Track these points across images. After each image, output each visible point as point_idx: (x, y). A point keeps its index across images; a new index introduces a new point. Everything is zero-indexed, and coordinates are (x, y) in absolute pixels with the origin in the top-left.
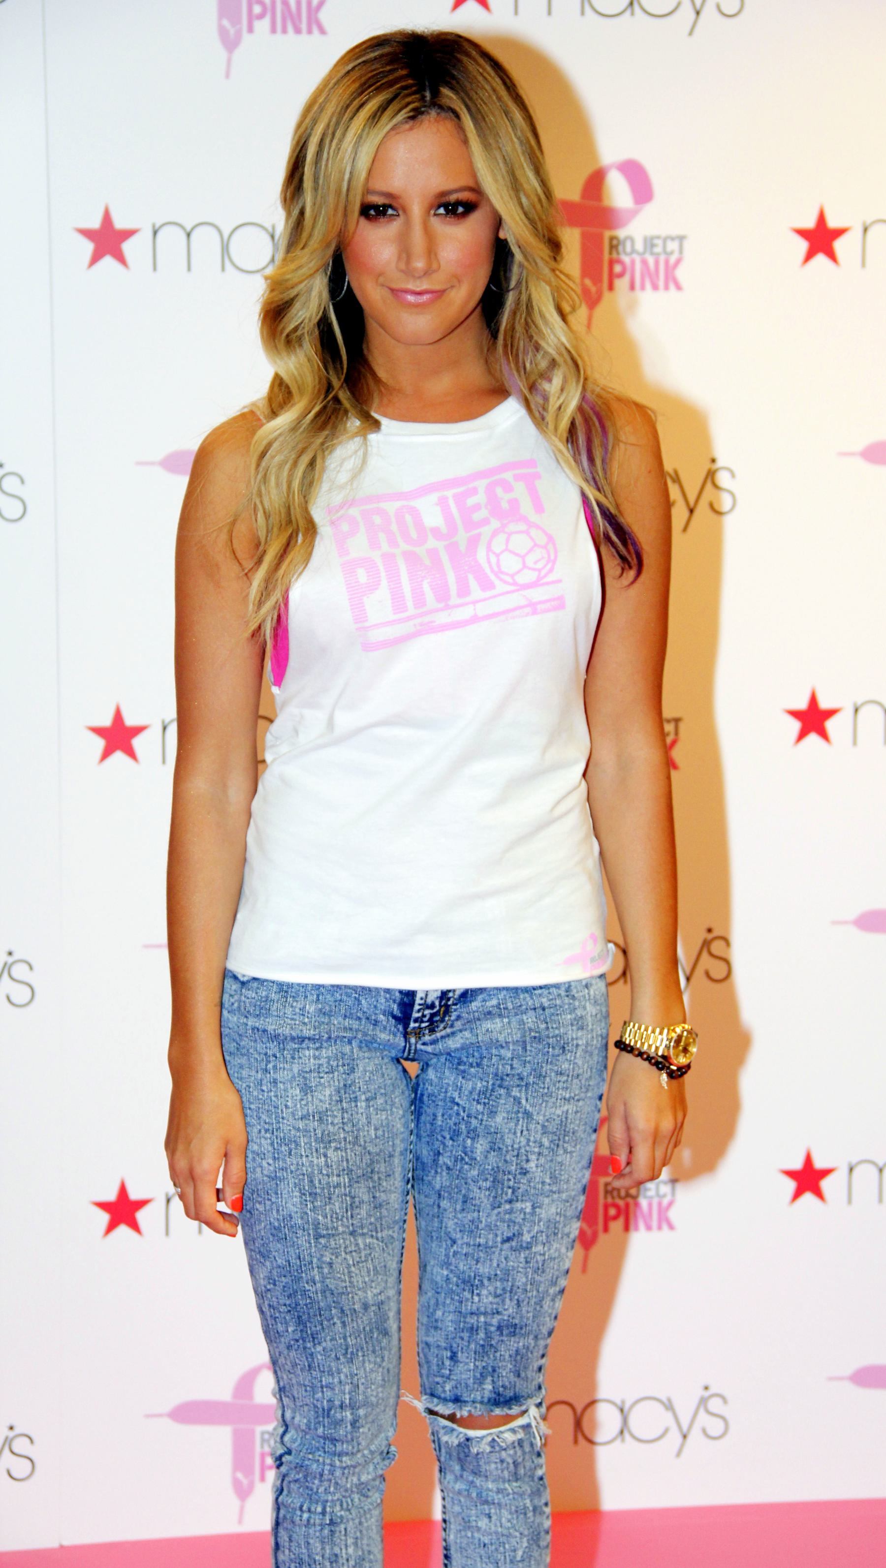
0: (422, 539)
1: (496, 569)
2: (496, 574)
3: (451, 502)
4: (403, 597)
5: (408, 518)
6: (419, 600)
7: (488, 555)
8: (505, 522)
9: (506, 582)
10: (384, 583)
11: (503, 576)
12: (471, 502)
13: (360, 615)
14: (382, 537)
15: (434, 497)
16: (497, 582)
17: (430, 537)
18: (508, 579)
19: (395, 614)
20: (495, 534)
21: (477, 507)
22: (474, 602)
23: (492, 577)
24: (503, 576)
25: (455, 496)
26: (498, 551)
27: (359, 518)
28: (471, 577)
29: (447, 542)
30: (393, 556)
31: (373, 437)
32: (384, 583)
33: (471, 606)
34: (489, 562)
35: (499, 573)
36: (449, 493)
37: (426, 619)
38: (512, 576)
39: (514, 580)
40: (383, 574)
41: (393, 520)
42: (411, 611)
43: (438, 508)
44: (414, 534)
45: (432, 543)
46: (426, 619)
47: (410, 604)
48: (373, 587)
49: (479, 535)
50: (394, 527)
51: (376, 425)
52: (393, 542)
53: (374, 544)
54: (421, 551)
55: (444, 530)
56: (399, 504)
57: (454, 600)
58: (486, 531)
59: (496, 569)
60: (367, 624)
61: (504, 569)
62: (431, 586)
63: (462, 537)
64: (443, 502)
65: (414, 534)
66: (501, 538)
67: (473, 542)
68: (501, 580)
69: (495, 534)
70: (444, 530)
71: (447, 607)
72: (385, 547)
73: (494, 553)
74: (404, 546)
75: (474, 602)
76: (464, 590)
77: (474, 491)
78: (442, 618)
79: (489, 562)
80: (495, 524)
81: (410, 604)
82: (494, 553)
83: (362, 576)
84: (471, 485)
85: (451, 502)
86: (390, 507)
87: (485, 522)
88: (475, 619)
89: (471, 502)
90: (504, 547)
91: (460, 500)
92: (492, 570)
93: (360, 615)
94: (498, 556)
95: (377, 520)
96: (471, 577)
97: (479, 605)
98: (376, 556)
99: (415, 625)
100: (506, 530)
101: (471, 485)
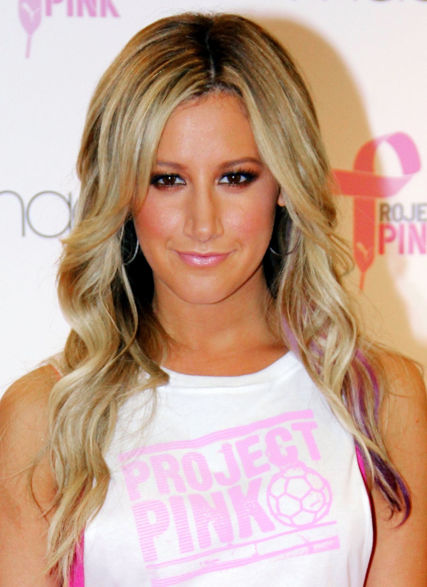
0: (207, 484)
1: (275, 511)
2: (275, 516)
3: (234, 450)
4: (190, 537)
5: (195, 465)
7: (268, 499)
9: (285, 524)
10: (172, 524)
11: (282, 518)
12: (252, 449)
13: (150, 553)
14: (170, 482)
15: (218, 445)
17: (215, 481)
18: (288, 521)
19: (182, 552)
20: (275, 478)
21: (258, 454)
22: (256, 542)
23: (272, 519)
24: (282, 518)
25: (237, 444)
26: (277, 494)
27: (149, 465)
29: (230, 487)
30: (181, 499)
31: (162, 389)
32: (172, 524)
33: (253, 546)
35: (278, 515)
36: (232, 441)
37: (211, 558)
38: (291, 518)
39: (292, 521)
41: (181, 466)
42: (197, 549)
43: (222, 456)
44: (200, 479)
45: (216, 487)
46: (211, 558)
47: (196, 544)
48: (162, 527)
49: (260, 480)
50: (181, 473)
51: (165, 378)
52: (180, 487)
53: (163, 488)
54: (206, 494)
55: (228, 475)
56: (185, 451)
57: (237, 540)
58: (266, 476)
59: (275, 511)
61: (283, 511)
62: (215, 527)
63: (244, 482)
64: (226, 449)
65: (200, 479)
66: (280, 484)
67: (255, 487)
68: (281, 522)
69: (275, 478)
70: (228, 475)
71: (231, 547)
72: (173, 491)
73: (274, 497)
74: (190, 490)
75: (256, 542)
76: (246, 531)
77: (256, 439)
78: (226, 557)
80: (275, 470)
81: (196, 544)
82: (274, 497)
83: (152, 518)
85: (234, 450)
86: (179, 454)
87: (265, 468)
88: (256, 558)
89: (252, 449)
90: (283, 491)
91: (242, 447)
92: (272, 513)
93: (150, 553)
94: (277, 499)
95: (166, 466)
97: (259, 545)
98: (165, 499)
99: (201, 563)
100: (285, 475)
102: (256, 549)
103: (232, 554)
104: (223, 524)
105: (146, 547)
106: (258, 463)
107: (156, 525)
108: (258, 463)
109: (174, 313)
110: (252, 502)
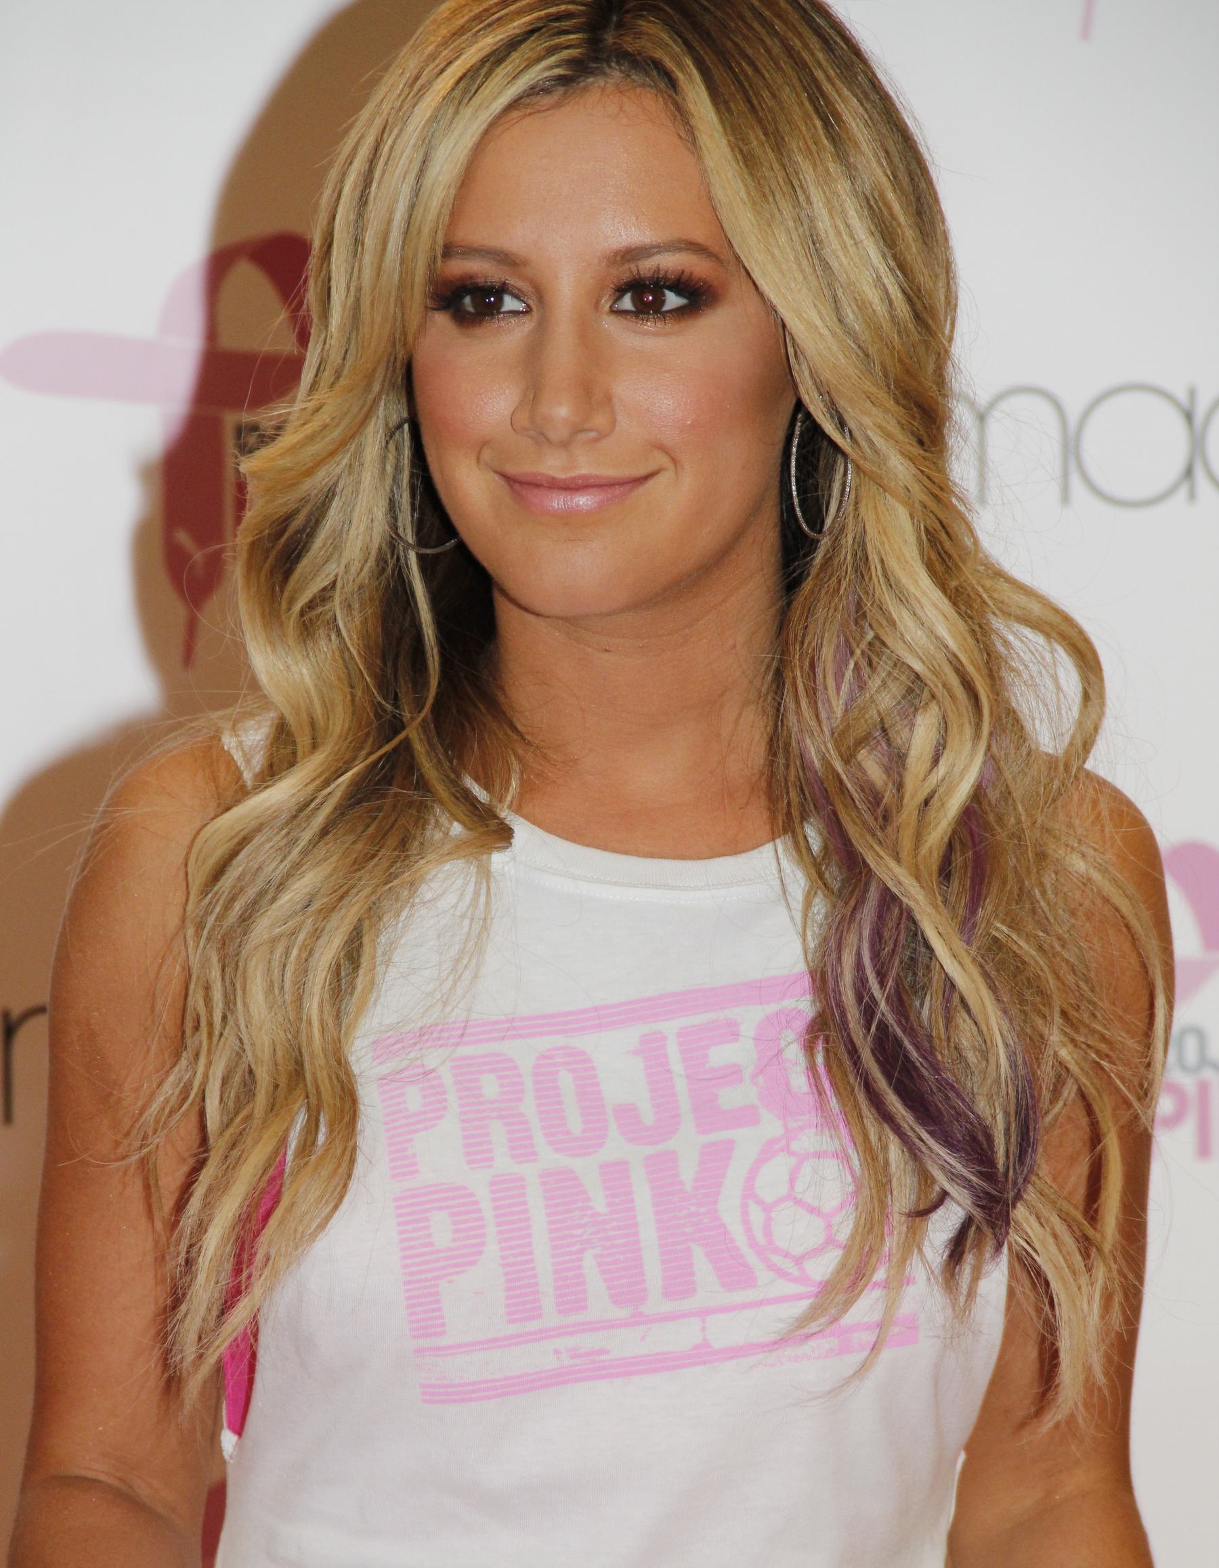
1: (761, 1239)
3: (673, 1050)
5: (566, 1081)
6: (571, 1295)
7: (744, 1206)
8: (793, 1125)
9: (782, 1274)
10: (492, 1248)
11: (777, 1259)
12: (721, 1055)
13: (426, 1318)
14: (498, 1132)
15: (630, 1036)
16: (763, 1275)
17: (613, 1125)
18: (788, 1266)
19: (511, 1322)
20: (767, 1153)
21: (732, 1074)
22: (704, 1313)
23: (752, 1259)
24: (777, 1259)
25: (681, 1034)
27: (447, 1078)
28: (698, 1252)
29: (650, 1150)
32: (492, 1248)
33: (696, 1322)
34: (746, 1222)
36: (670, 1027)
37: (588, 1341)
39: (802, 1270)
40: (491, 1230)
42: (551, 1317)
44: (575, 1124)
45: (615, 1147)
46: (588, 1341)
47: (548, 1302)
49: (729, 1145)
50: (529, 1106)
51: (504, 835)
52: (522, 1149)
53: (477, 1152)
54: (587, 1169)
55: (648, 1116)
56: (543, 1043)
57: (656, 1304)
58: (747, 1141)
59: (761, 1239)
60: (442, 1341)
62: (600, 1264)
63: (687, 1144)
64: (651, 1049)
65: (575, 1124)
66: (779, 1167)
67: (716, 1159)
68: (772, 1267)
69: (767, 1153)
70: (648, 1116)
71: (639, 1319)
72: (503, 1162)
73: (760, 1202)
74: (549, 1157)
75: (704, 1313)
76: (679, 1283)
77: (731, 1032)
79: (746, 1222)
80: (770, 1126)
81: (548, 1302)
82: (760, 1202)
83: (441, 1230)
84: (725, 1014)
85: (673, 1050)
86: (524, 1053)
87: (746, 1116)
88: (703, 1355)
89: (721, 1055)
90: (783, 1190)
92: (753, 1244)
94: (767, 1209)
95: (490, 1087)
96: (698, 1252)
98: (478, 1182)
99: (557, 1352)
100: (795, 1146)
101: (725, 1014)
102: (703, 1329)
103: (643, 1339)
104: (622, 1257)
105: (419, 1305)
106: (732, 1097)
107: (450, 1249)
108: (732, 1097)
109: (541, 668)
110: (703, 1210)
